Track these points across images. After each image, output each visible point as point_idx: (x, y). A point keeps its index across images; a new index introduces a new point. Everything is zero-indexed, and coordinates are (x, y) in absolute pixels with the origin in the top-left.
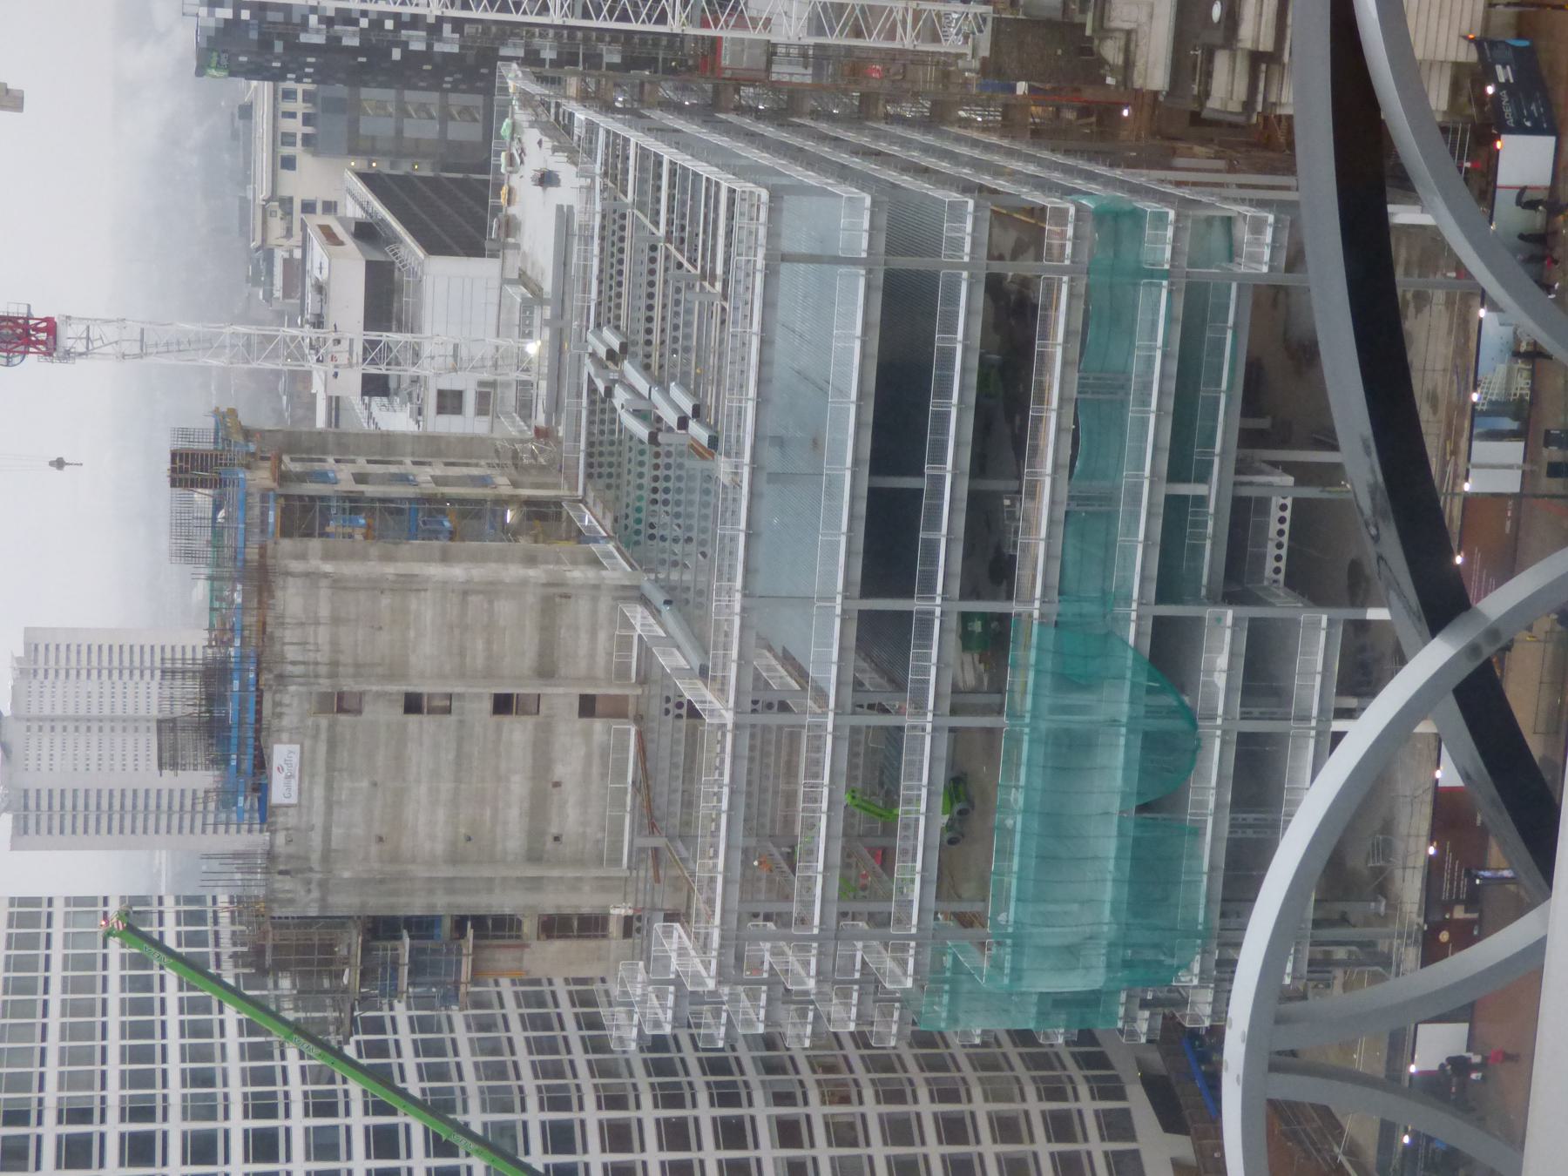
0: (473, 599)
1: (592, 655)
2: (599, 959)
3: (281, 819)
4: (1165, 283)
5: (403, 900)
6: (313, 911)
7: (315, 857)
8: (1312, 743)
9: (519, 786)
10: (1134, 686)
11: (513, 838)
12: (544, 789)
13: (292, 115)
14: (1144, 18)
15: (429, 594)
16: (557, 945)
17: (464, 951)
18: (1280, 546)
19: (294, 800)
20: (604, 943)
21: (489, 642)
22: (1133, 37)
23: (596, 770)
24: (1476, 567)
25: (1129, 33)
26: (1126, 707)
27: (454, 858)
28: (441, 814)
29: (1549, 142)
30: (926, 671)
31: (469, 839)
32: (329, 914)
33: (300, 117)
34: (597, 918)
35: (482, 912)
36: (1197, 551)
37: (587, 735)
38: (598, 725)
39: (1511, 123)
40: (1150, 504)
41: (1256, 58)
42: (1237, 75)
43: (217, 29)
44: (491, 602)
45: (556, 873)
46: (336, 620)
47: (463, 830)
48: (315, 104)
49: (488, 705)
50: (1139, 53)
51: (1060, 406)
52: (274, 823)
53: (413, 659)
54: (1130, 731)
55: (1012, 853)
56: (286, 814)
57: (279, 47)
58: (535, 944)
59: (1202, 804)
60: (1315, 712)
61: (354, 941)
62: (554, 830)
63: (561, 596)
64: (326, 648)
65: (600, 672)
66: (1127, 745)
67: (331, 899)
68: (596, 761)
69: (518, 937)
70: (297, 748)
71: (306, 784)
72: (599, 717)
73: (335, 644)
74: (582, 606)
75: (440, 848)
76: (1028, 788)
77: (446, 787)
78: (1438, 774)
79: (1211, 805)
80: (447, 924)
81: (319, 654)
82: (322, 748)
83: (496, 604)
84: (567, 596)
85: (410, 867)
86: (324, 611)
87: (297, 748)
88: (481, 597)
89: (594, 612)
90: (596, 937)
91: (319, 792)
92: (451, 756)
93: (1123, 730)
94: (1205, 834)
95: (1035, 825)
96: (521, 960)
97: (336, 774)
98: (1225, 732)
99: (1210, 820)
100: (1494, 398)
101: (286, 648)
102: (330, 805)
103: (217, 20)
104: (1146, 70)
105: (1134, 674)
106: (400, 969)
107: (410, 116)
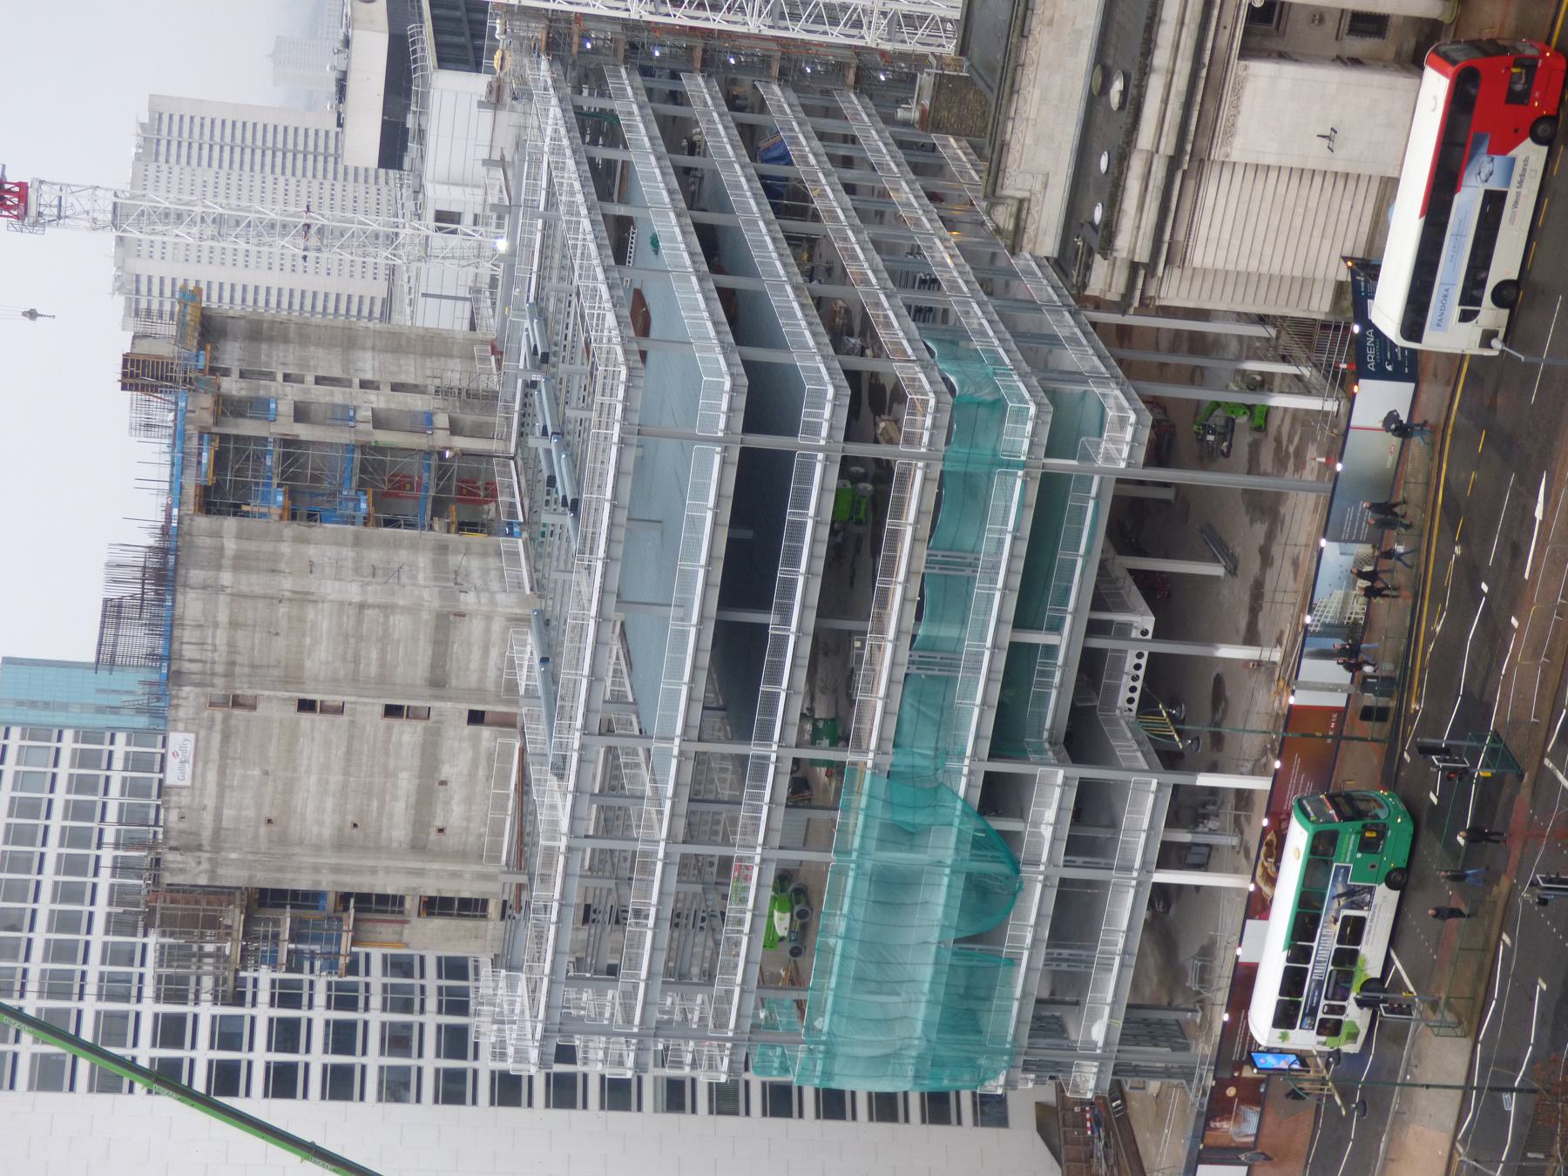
0: (369, 612)
1: (483, 670)
2: (476, 937)
3: (174, 799)
4: (1020, 473)
5: (289, 876)
6: (203, 880)
7: (206, 835)
8: (1132, 891)
9: (406, 782)
10: (960, 831)
11: (399, 830)
12: (430, 786)
14: (1038, 187)
15: (326, 605)
16: (437, 923)
17: (345, 928)
18: (1135, 678)
19: (188, 782)
20: (482, 923)
21: (383, 652)
22: (1026, 205)
23: (481, 773)
24: (1295, 770)
25: (1021, 201)
26: (951, 852)
27: (341, 845)
28: (330, 803)
29: (1410, 386)
30: (758, 809)
31: (355, 825)
32: (218, 884)
34: (477, 900)
35: (365, 890)
36: (1043, 699)
37: (476, 740)
38: (486, 732)
39: (1371, 367)
40: (990, 670)
41: (1134, 267)
42: (1116, 270)
44: (386, 617)
45: (436, 866)
46: (234, 625)
47: (350, 818)
49: (381, 710)
50: (1030, 219)
51: (907, 580)
52: (169, 801)
53: (308, 664)
54: (953, 872)
55: (831, 973)
56: (179, 794)
58: (415, 920)
59: (1022, 939)
60: (1137, 864)
61: (237, 918)
62: (439, 823)
63: (455, 615)
64: (223, 648)
65: (490, 685)
66: (949, 886)
67: (220, 871)
68: (483, 763)
69: (401, 912)
70: (192, 736)
72: (488, 725)
73: (232, 646)
74: (476, 626)
75: (327, 833)
76: (850, 918)
77: (335, 779)
78: (1239, 951)
79: (1029, 940)
80: (331, 899)
81: (216, 655)
84: (461, 615)
85: (297, 850)
86: (223, 617)
88: (377, 611)
89: (487, 631)
90: (475, 916)
91: (212, 776)
92: (343, 750)
93: (947, 871)
94: (1020, 965)
95: (854, 951)
96: (401, 934)
97: (229, 762)
98: (1046, 878)
99: (1026, 954)
100: (1328, 621)
101: (185, 647)
102: (222, 788)
104: (1036, 236)
105: (961, 823)
106: (281, 944)
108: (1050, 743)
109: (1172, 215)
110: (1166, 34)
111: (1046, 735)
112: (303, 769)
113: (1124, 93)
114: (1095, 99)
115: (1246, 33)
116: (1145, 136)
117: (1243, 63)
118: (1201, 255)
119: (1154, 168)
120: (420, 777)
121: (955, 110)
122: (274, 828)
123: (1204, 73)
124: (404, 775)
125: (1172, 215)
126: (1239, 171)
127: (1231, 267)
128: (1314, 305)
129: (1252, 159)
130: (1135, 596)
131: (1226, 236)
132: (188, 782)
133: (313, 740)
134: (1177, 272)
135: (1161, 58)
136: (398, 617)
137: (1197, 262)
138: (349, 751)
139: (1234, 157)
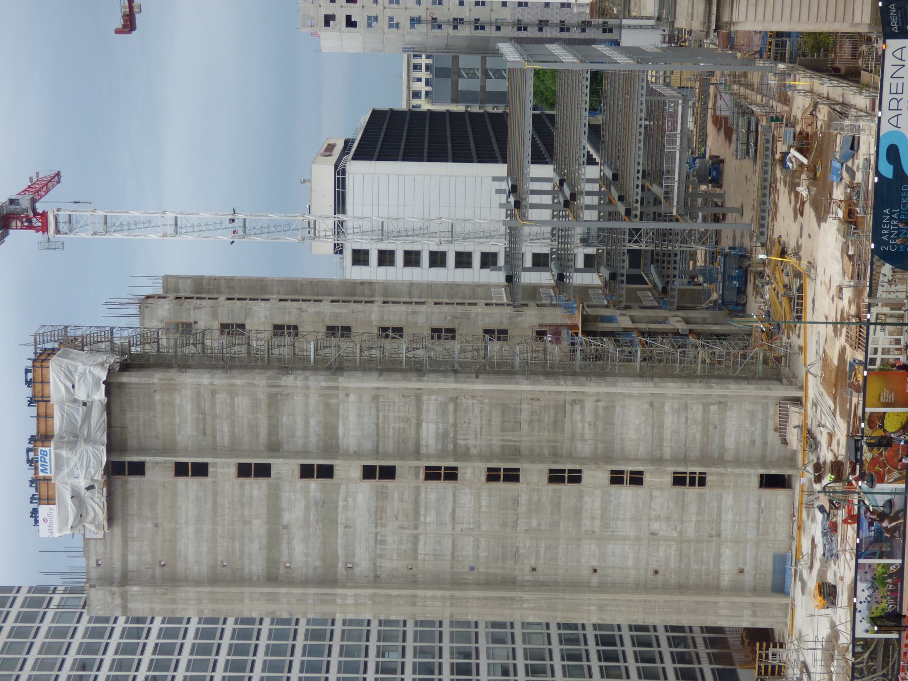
1: (306, 437)
9: (259, 527)
13: (419, 80)
28: (204, 547)
33: (424, 80)
37: (306, 491)
39: (895, 29)
44: (232, 399)
47: (220, 558)
48: (431, 72)
49: (233, 470)
53: (179, 438)
75: (205, 570)
77: (207, 527)
83: (236, 399)
89: (306, 405)
107: (489, 77)
112: (183, 521)
120: (268, 523)
122: (166, 569)
124: (256, 522)
128: (857, 19)
133: (188, 498)
136: (240, 398)
138: (215, 505)
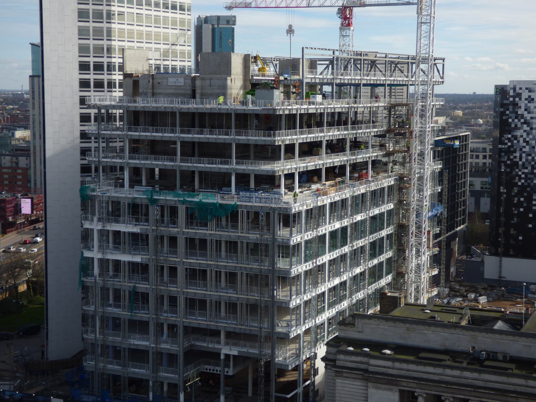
14: (359, 330)
18: (213, 370)
22: (353, 326)
25: (354, 325)
36: (204, 341)
42: (334, 356)
43: (506, 90)
50: (349, 328)
57: (502, 110)
70: (183, 84)
71: (173, 87)
82: (182, 92)
87: (183, 84)
91: (171, 91)
103: (509, 91)
104: (344, 330)
108: (191, 345)
109: (350, 372)
110: (404, 366)
111: (193, 342)
113: (385, 354)
114: (386, 346)
115: (409, 391)
116: (373, 362)
117: (398, 391)
118: (339, 381)
119: (365, 365)
121: (387, 303)
123: (394, 379)
125: (350, 372)
126: (365, 392)
127: (337, 391)
129: (369, 395)
130: (238, 369)
131: (346, 389)
132: (169, 84)
134: (334, 374)
135: (397, 365)
137: (338, 381)
139: (369, 389)
